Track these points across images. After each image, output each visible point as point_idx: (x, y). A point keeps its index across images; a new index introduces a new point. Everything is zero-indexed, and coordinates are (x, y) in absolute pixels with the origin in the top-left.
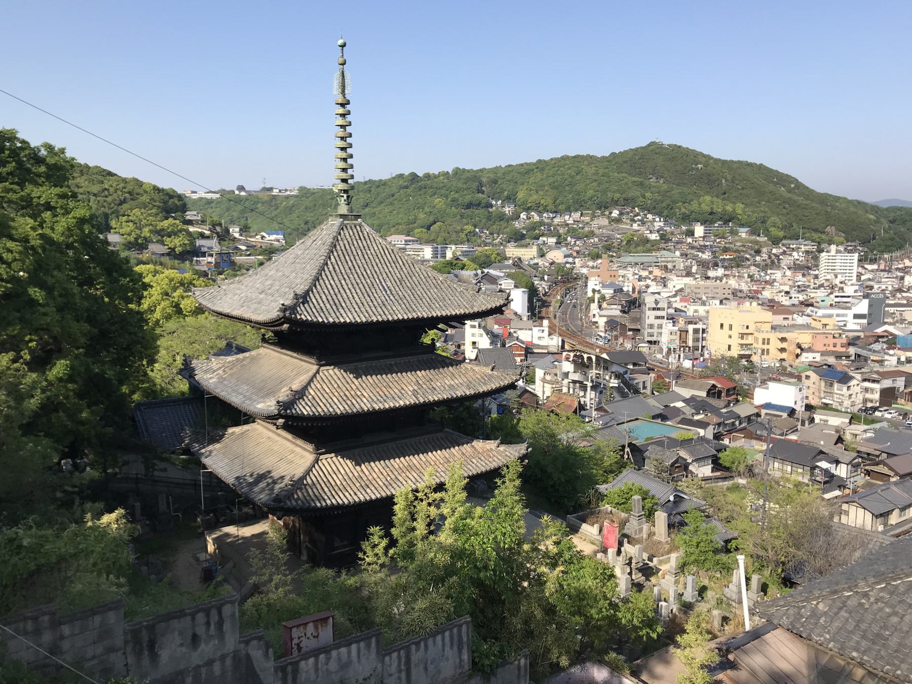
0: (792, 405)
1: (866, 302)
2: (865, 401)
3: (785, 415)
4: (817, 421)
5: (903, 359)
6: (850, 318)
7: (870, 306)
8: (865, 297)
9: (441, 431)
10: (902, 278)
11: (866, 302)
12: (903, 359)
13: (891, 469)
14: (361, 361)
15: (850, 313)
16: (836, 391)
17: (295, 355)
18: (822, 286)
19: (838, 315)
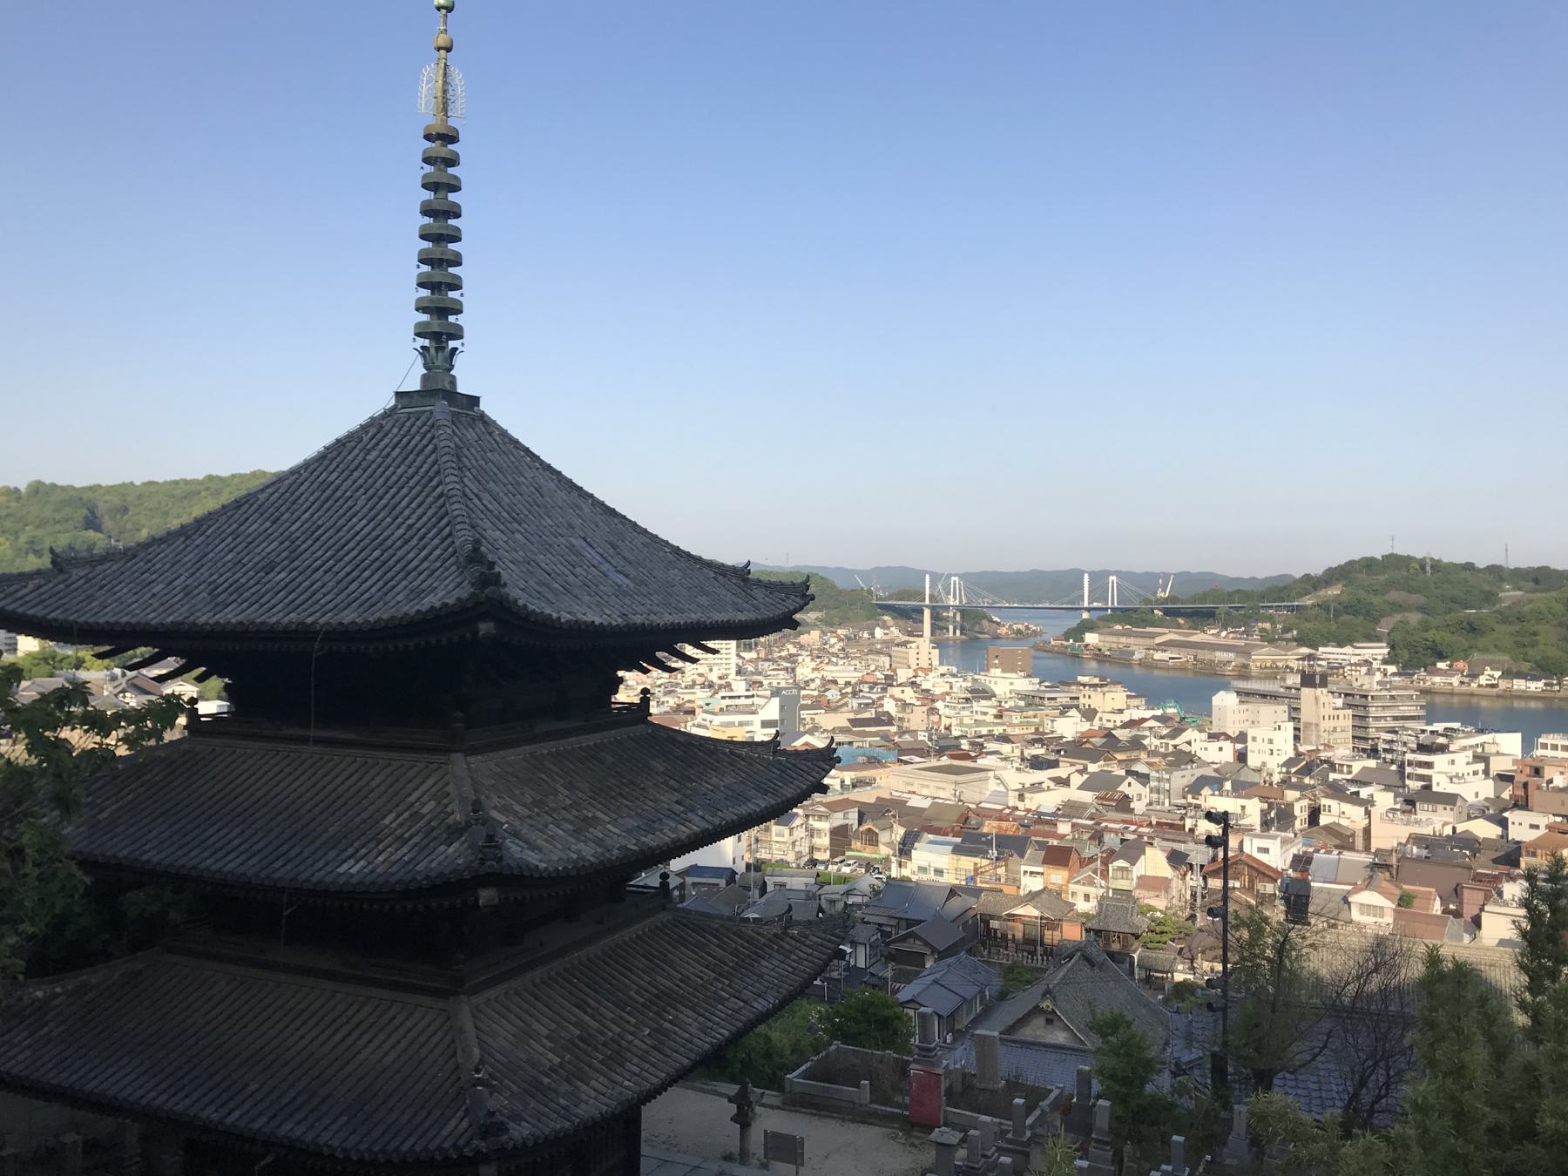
0: (729, 864)
1: (776, 701)
2: (812, 849)
3: (722, 883)
4: (770, 888)
5: (848, 782)
6: (757, 727)
7: (782, 708)
8: (773, 695)
9: (664, 909)
10: (793, 670)
11: (776, 701)
12: (848, 782)
13: (927, 944)
14: (533, 740)
15: (756, 720)
16: (775, 838)
17: (351, 736)
18: (694, 684)
19: (741, 724)
